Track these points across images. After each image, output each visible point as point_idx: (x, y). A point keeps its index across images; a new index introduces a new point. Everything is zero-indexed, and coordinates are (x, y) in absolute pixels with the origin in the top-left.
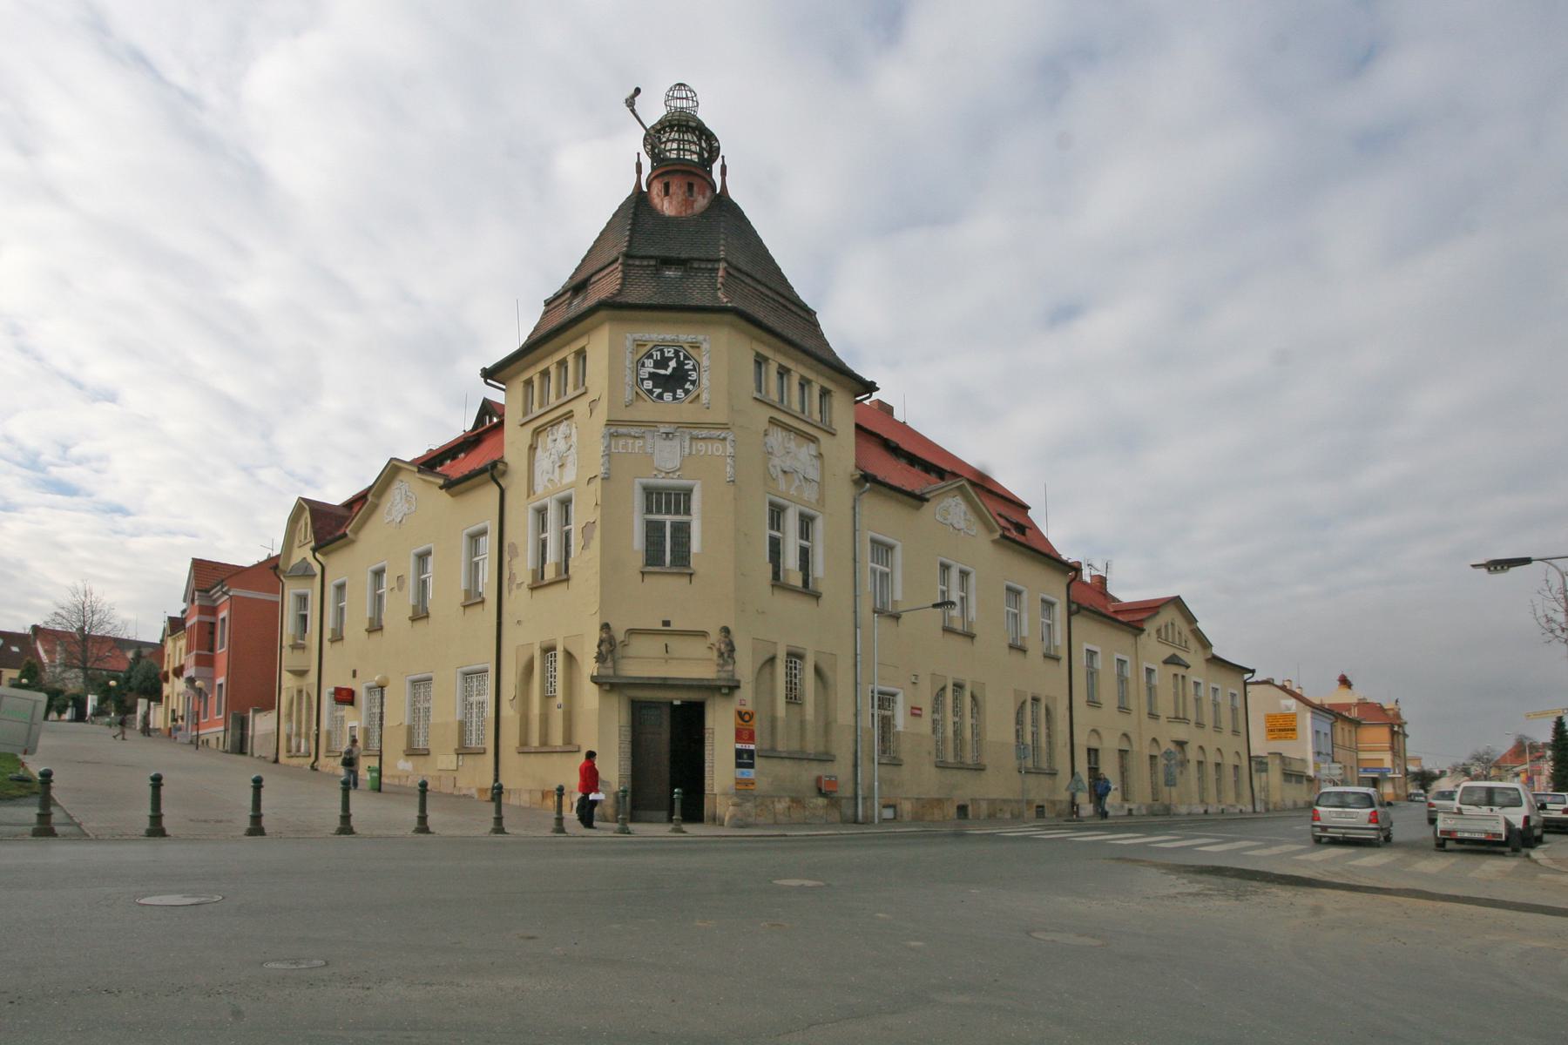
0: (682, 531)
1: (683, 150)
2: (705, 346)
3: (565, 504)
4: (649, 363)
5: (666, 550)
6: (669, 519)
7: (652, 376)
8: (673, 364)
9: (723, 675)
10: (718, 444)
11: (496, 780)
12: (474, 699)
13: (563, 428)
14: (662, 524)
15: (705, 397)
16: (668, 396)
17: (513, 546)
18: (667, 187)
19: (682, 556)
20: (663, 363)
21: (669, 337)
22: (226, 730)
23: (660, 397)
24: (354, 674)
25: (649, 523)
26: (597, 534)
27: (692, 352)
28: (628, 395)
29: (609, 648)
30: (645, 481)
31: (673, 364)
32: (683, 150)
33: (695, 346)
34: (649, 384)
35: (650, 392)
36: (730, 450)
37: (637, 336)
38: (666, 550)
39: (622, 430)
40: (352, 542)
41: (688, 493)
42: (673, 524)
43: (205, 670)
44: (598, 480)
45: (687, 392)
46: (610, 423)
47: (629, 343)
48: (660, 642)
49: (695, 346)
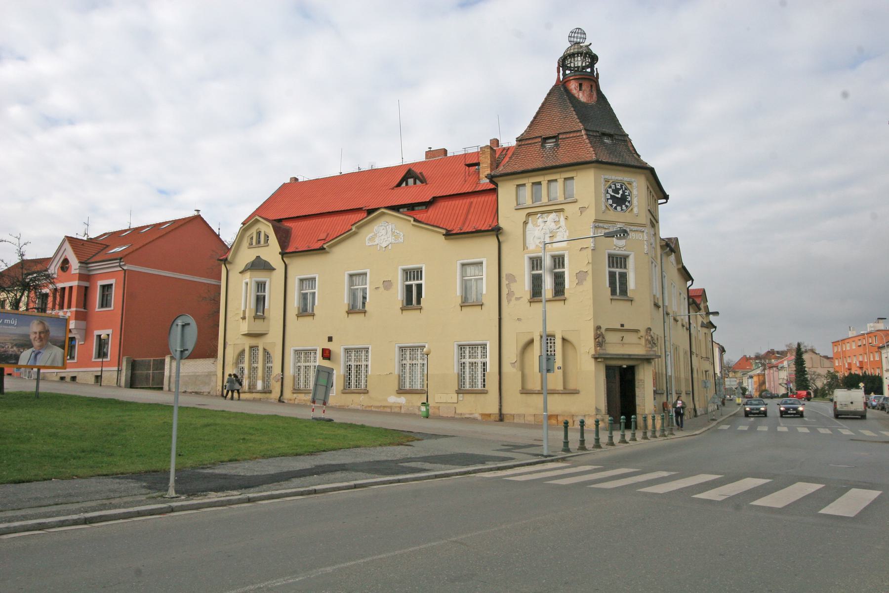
0: (623, 276)
1: (579, 67)
2: (634, 184)
3: (558, 261)
4: (610, 191)
5: (618, 286)
6: (618, 271)
7: (612, 197)
8: (621, 192)
9: (652, 353)
10: (640, 234)
11: (500, 410)
12: (467, 360)
13: (553, 216)
14: (615, 273)
15: (635, 210)
16: (619, 208)
17: (512, 278)
18: (581, 85)
19: (624, 291)
20: (616, 191)
21: (620, 178)
22: (119, 371)
23: (615, 208)
24: (330, 339)
25: (610, 272)
26: (589, 278)
27: (629, 186)
28: (604, 208)
29: (600, 338)
30: (610, 251)
31: (621, 192)
32: (579, 67)
33: (630, 183)
34: (610, 202)
35: (611, 205)
36: (646, 238)
37: (607, 177)
38: (618, 286)
39: (601, 225)
40: (328, 252)
41: (625, 258)
42: (620, 274)
43: (83, 324)
44: (589, 251)
45: (627, 206)
46: (596, 221)
47: (602, 180)
48: (620, 334)
49: (630, 183)
